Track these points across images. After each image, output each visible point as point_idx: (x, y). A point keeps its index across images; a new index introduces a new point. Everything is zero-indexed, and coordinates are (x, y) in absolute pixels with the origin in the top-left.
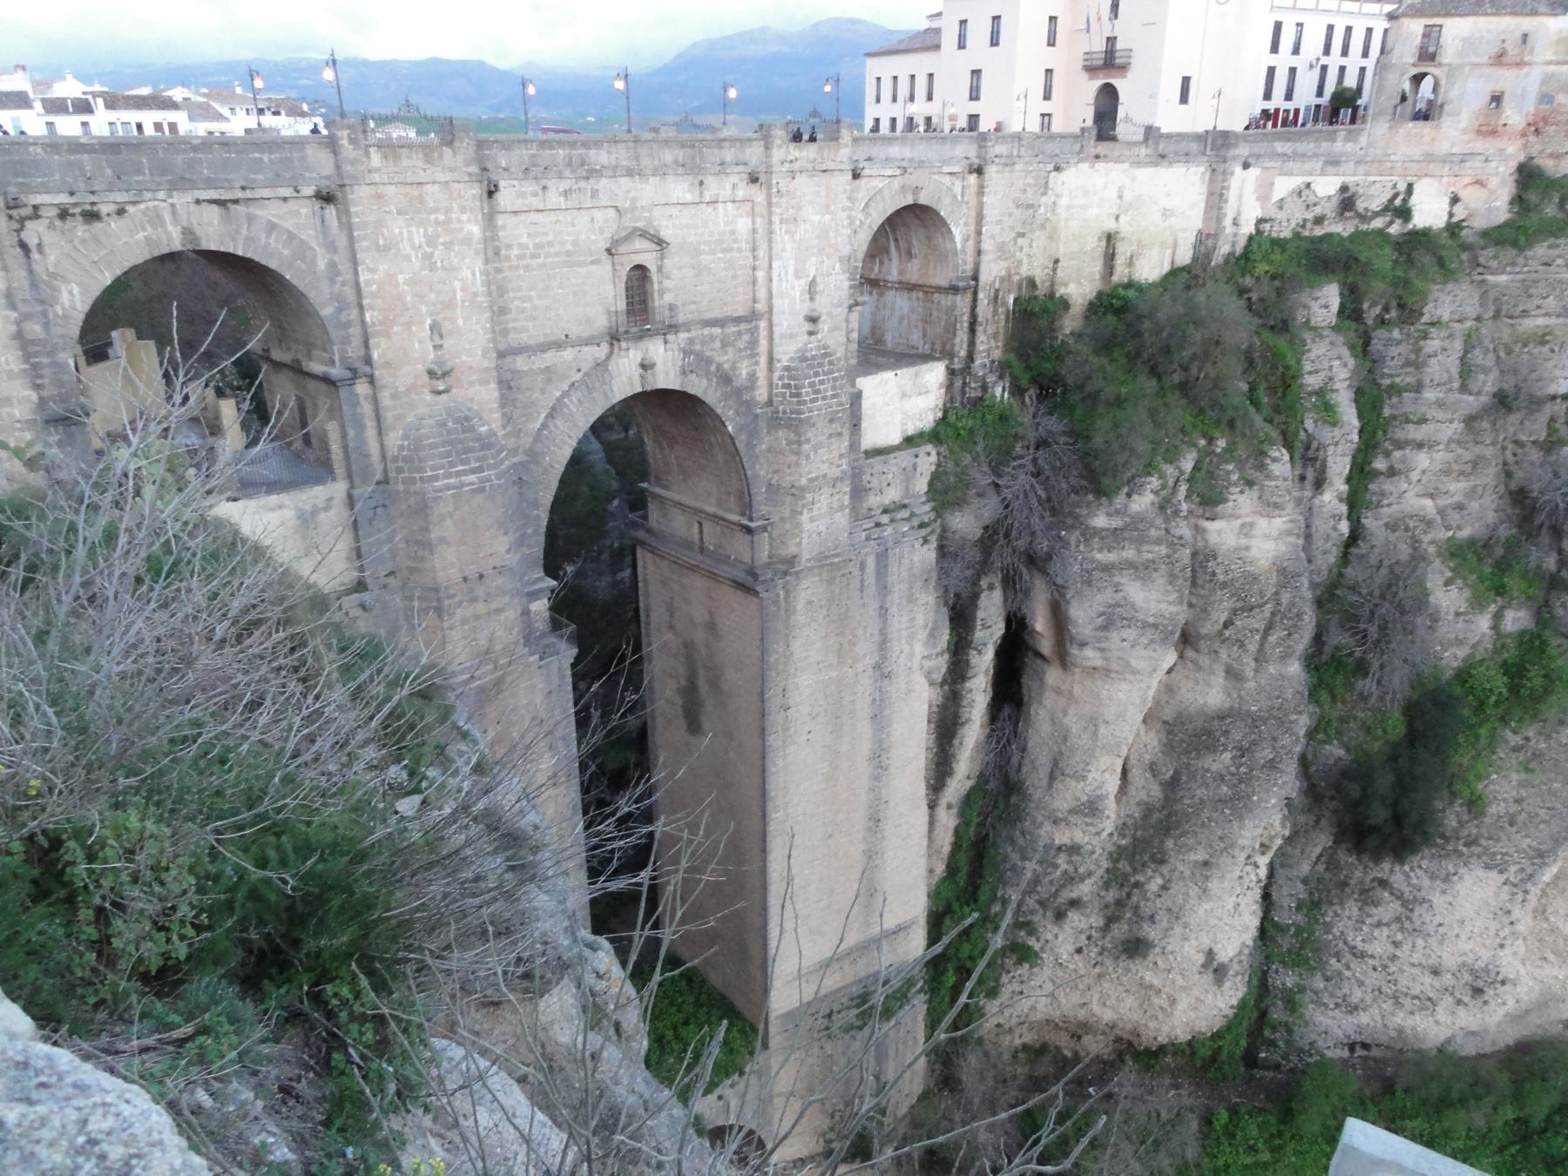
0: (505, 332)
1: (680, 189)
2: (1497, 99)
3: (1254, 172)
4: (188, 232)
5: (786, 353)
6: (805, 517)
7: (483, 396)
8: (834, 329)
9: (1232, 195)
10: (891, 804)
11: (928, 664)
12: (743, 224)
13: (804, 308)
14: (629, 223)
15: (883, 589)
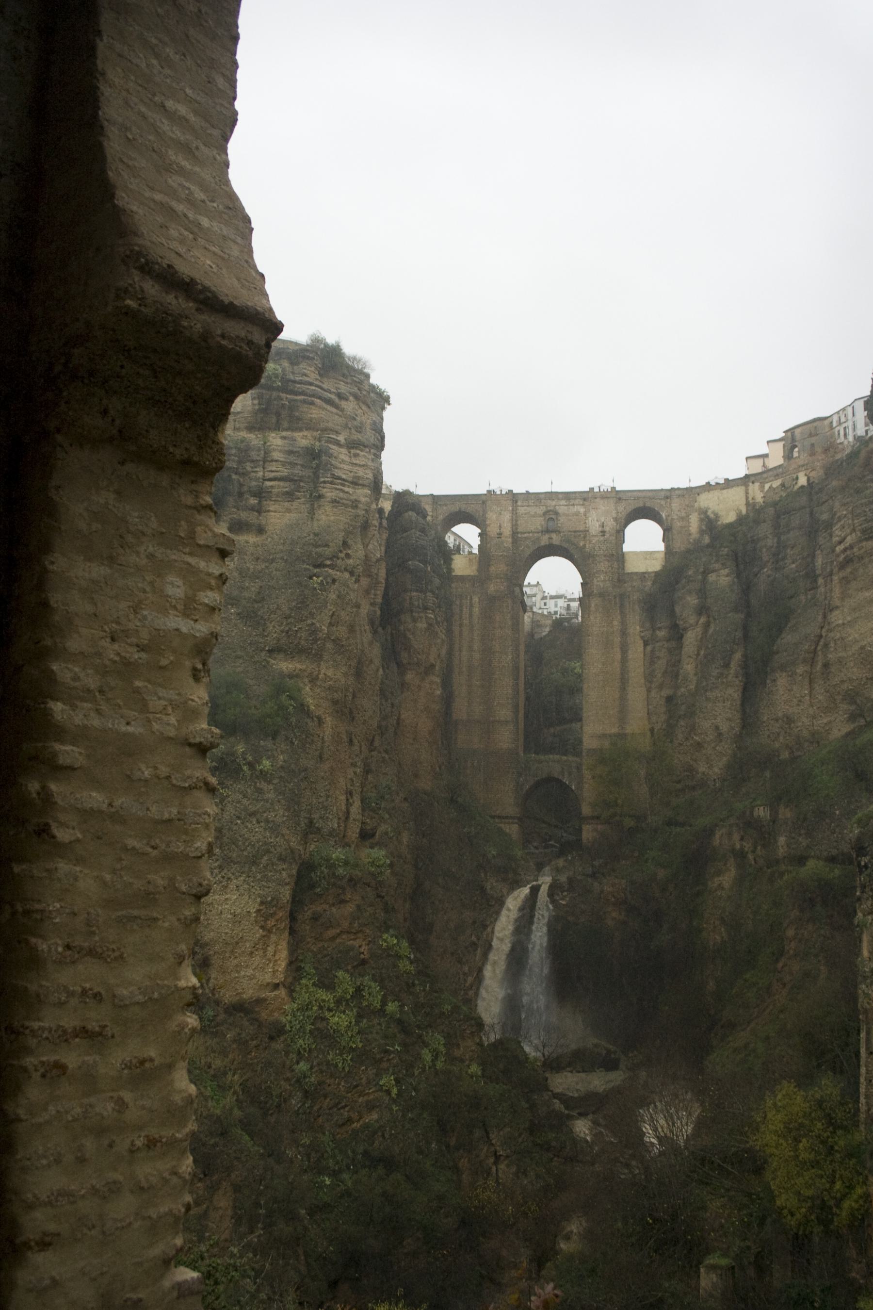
0: (517, 529)
1: (563, 502)
2: (813, 445)
3: (757, 485)
4: (460, 508)
5: (594, 541)
6: (595, 580)
7: (508, 542)
8: (610, 536)
9: (750, 491)
10: (630, 681)
11: (642, 634)
12: (582, 510)
13: (600, 529)
14: (549, 508)
15: (622, 606)
